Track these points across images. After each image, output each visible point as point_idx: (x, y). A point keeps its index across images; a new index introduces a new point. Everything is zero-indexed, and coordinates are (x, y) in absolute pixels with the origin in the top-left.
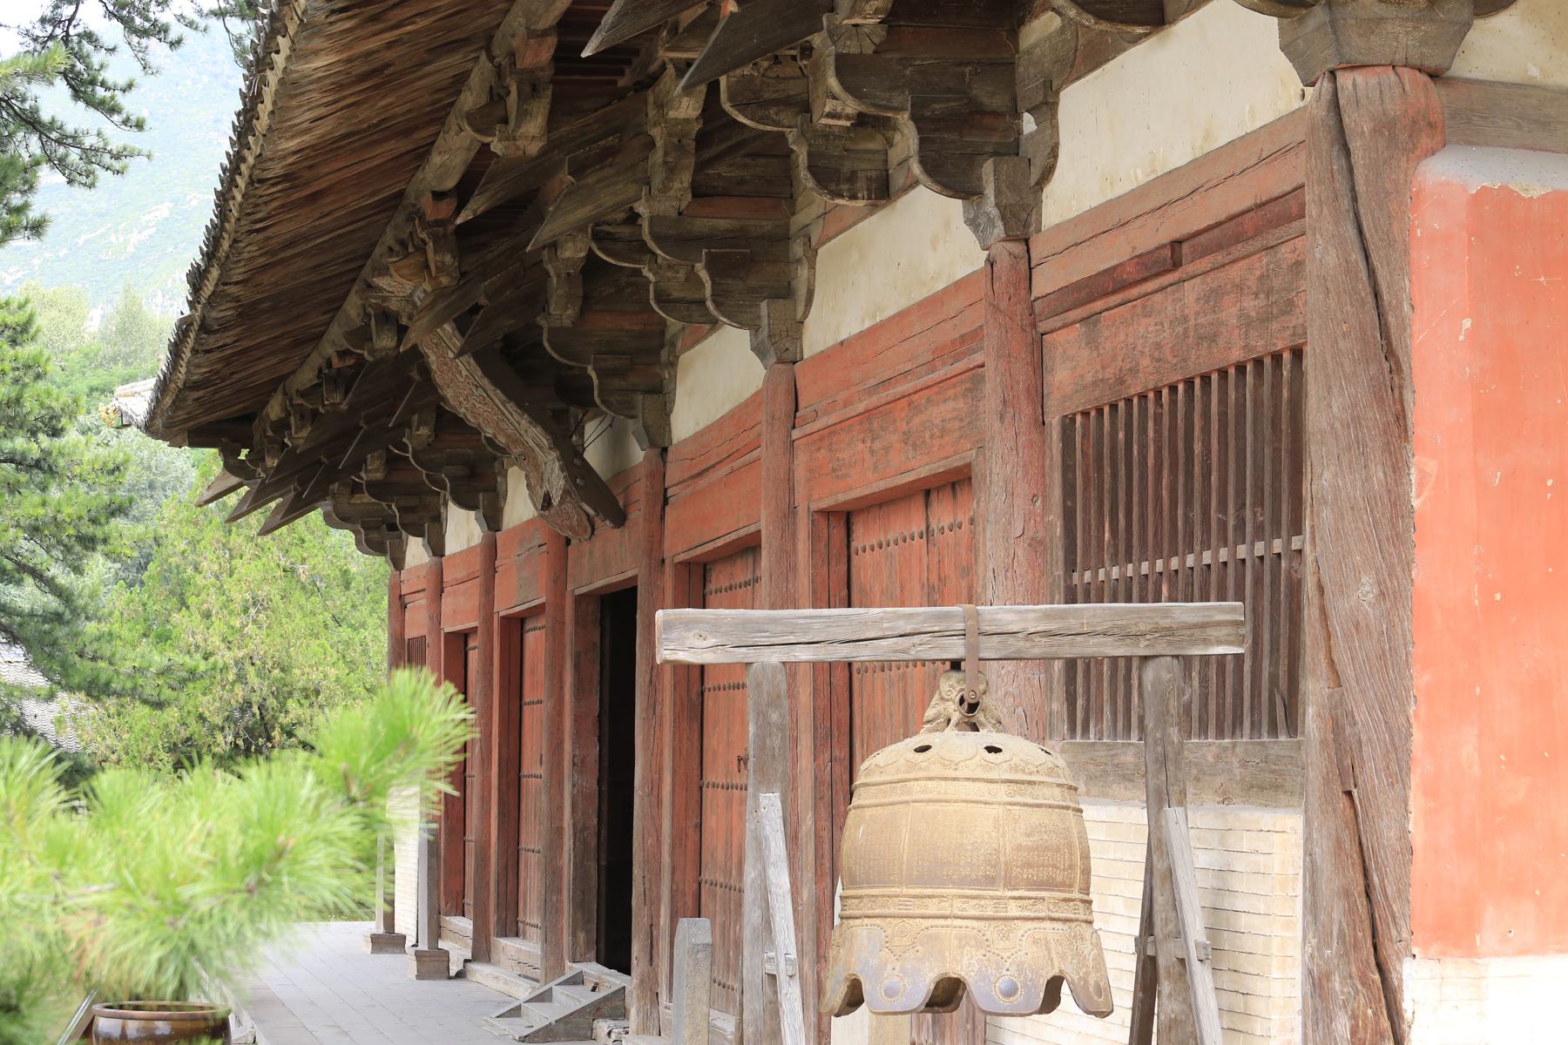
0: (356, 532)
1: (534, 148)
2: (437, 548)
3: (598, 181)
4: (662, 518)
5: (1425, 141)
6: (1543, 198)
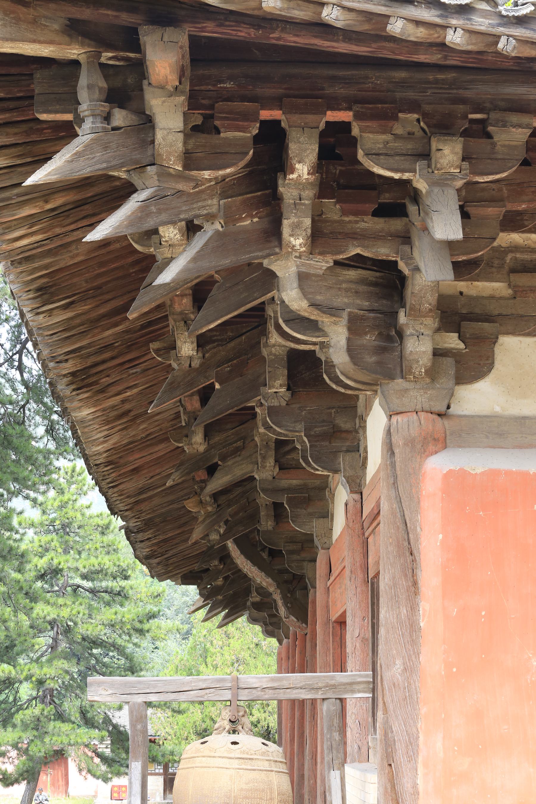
1: (202, 449)
3: (234, 463)
5: (431, 447)
6: (482, 473)
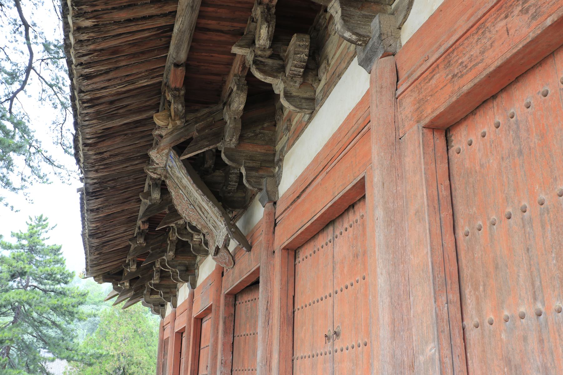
0: (151, 307)
2: (175, 306)
4: (274, 233)
